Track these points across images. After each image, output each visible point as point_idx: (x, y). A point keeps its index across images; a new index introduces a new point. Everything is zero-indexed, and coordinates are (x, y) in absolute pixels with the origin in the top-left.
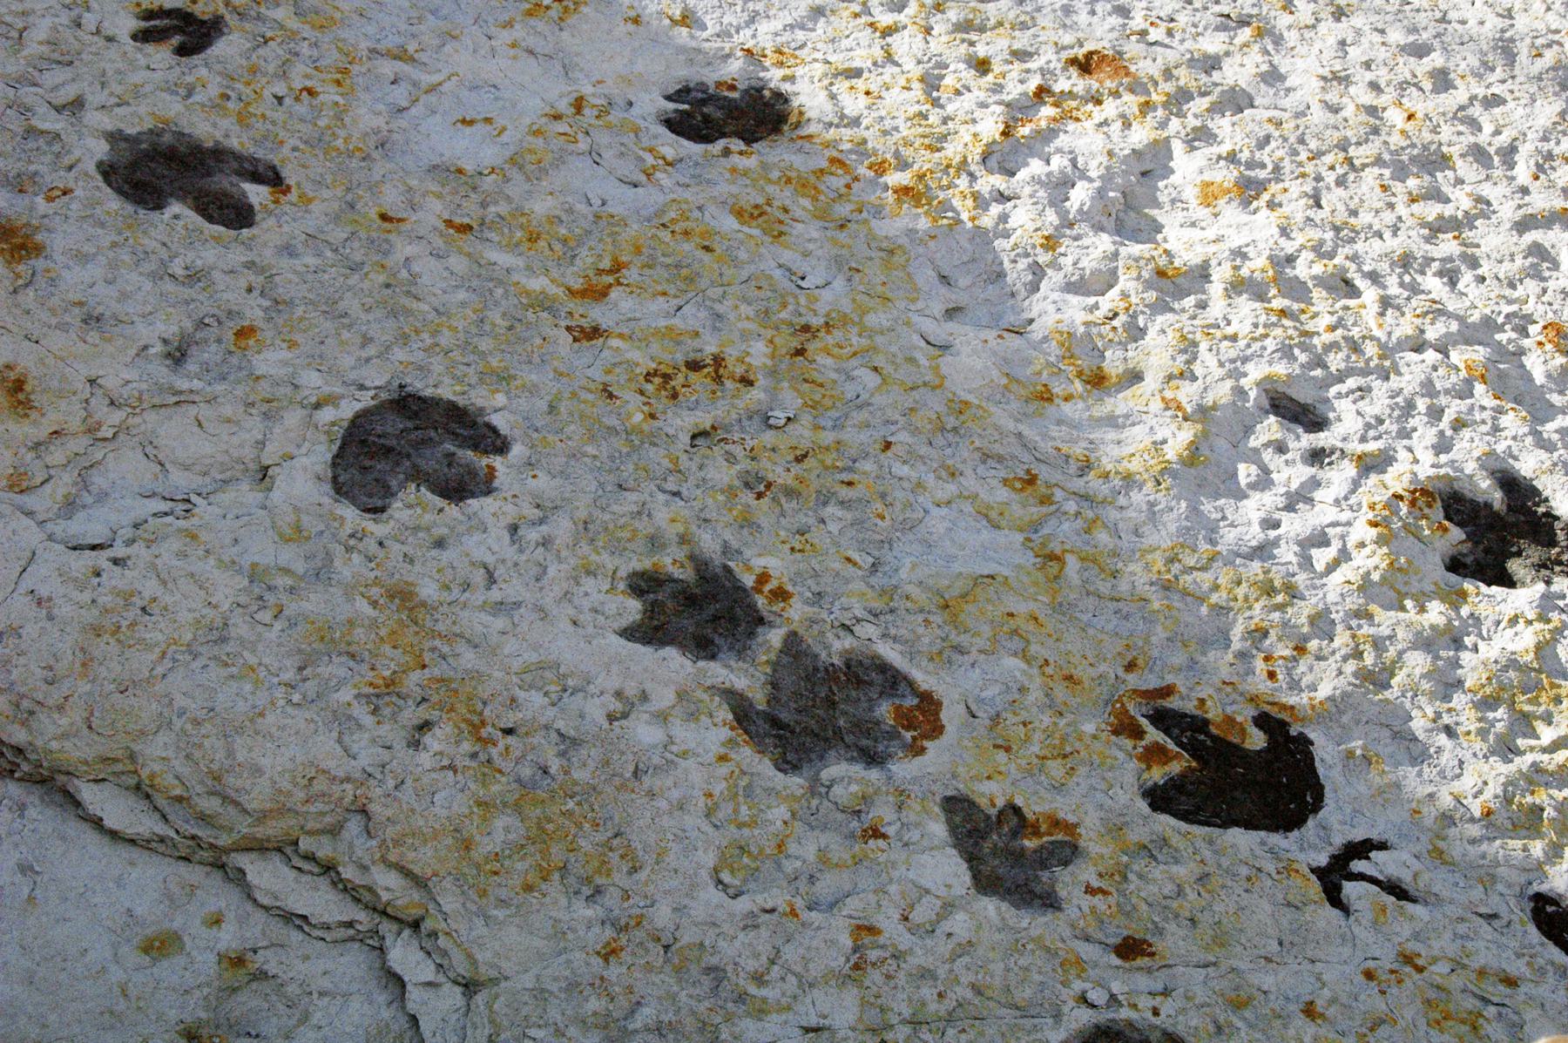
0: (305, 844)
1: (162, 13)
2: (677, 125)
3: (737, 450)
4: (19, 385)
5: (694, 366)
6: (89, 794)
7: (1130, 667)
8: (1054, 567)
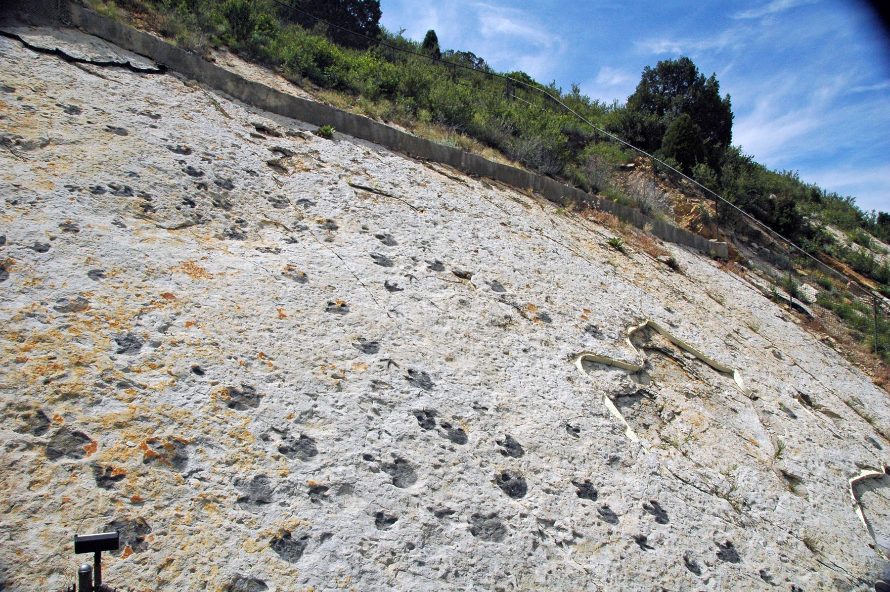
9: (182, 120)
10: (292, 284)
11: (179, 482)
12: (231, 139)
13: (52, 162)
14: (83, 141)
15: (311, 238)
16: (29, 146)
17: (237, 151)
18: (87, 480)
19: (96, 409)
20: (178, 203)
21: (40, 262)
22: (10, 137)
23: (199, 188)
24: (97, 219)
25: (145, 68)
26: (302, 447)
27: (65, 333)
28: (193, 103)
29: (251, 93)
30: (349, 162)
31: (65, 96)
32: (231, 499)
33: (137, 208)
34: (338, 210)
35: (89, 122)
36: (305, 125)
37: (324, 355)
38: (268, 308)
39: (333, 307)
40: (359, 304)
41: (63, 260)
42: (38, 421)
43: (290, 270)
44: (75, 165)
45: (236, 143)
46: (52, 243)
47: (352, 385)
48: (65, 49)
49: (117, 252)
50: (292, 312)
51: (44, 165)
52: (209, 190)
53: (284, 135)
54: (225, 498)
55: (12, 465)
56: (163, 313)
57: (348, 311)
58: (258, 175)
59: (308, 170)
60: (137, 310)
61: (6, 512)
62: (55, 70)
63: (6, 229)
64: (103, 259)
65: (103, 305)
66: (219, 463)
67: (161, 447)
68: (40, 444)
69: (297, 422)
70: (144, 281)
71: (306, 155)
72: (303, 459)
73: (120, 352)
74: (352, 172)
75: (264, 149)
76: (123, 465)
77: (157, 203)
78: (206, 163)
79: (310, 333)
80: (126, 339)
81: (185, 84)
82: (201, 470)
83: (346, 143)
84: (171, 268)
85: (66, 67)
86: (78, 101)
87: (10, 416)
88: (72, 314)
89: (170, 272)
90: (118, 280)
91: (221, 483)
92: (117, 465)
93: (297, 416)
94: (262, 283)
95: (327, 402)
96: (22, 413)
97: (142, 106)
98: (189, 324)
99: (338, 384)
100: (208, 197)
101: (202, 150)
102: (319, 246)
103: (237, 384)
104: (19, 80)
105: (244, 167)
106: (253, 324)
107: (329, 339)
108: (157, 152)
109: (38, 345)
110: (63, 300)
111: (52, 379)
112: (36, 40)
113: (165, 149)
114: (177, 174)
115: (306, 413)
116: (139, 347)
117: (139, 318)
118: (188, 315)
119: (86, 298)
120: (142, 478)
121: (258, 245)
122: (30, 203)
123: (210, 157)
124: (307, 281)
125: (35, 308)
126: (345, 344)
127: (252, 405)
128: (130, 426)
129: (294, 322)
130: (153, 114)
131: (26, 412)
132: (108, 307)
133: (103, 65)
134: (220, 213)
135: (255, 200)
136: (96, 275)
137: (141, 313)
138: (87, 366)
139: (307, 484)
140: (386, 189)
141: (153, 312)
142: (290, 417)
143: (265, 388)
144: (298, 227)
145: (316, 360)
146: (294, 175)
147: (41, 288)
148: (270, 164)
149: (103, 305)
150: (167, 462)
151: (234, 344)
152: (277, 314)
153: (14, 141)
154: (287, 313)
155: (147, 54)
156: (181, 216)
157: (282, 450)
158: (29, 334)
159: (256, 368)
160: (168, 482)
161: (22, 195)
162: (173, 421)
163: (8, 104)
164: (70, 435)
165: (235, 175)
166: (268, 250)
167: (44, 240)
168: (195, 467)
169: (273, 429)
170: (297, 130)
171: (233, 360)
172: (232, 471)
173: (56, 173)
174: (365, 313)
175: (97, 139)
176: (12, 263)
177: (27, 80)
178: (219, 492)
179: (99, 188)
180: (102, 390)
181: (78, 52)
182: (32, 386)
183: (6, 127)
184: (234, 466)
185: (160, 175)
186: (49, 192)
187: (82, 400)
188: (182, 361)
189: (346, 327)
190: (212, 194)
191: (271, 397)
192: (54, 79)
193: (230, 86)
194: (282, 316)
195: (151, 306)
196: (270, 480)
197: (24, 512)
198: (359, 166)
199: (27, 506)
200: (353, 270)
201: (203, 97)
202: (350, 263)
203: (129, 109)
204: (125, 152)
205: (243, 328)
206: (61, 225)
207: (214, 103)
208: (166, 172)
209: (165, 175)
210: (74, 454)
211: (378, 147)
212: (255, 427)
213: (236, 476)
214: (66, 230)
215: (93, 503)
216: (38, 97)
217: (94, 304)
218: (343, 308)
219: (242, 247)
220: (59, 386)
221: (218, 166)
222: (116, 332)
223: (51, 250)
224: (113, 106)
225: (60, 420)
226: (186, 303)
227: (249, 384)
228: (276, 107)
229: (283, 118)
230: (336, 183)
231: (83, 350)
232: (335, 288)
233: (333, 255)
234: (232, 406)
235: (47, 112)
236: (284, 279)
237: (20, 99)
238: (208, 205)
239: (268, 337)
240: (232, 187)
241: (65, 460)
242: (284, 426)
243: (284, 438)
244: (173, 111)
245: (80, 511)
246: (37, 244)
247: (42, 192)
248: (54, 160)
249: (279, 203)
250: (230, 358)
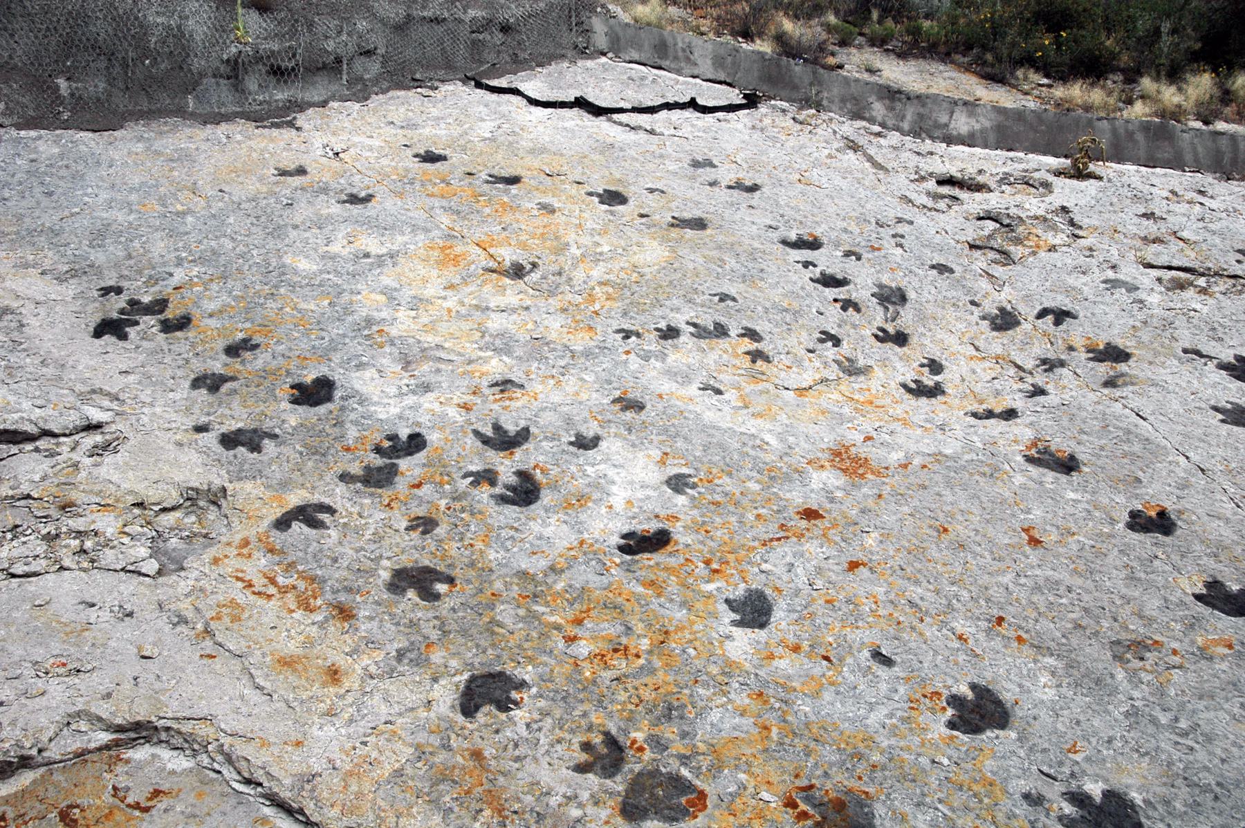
1: (418, 518)
2: (623, 549)
3: (629, 686)
4: (336, 672)
5: (616, 651)
7: (797, 776)
8: (765, 733)
29: (921, 116)
53: (993, 185)
59: (1052, 249)
112: (534, 85)
155: (722, 77)
156: (818, 364)
193: (878, 109)
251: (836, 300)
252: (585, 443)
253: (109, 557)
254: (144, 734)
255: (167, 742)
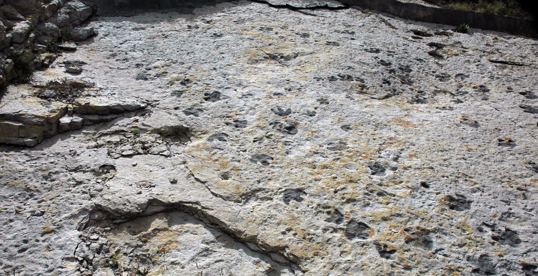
0: (279, 251)
6: (248, 244)
9: (368, 34)
10: (470, 130)
11: (431, 256)
12: (401, 41)
13: (302, 65)
14: (316, 52)
15: (472, 99)
16: (288, 58)
17: (407, 48)
18: (373, 252)
19: (368, 209)
20: (380, 83)
21: (313, 122)
22: (276, 55)
23: (390, 73)
24: (337, 95)
25: (336, 6)
26: (509, 237)
27: (338, 163)
28: (371, 23)
30: (485, 46)
31: (299, 28)
32: (468, 270)
33: (357, 88)
34: (486, 79)
35: (316, 41)
36: (446, 27)
37: (507, 174)
38: (459, 145)
39: (502, 142)
40: (522, 140)
41: (325, 121)
42: (336, 215)
43: (465, 120)
44: (316, 66)
45: (405, 43)
46: (316, 111)
47: (534, 195)
48: (290, 4)
49: (354, 114)
50: (475, 147)
51: (299, 68)
52: (397, 73)
54: (463, 268)
55: (328, 241)
56: (393, 150)
57: (515, 145)
58: (425, 62)
59: (457, 55)
60: (376, 148)
61: (332, 269)
62: (288, 16)
63: (289, 105)
64: (348, 119)
65: (356, 146)
66: (454, 245)
67: (414, 234)
68: (341, 229)
69: (500, 219)
70: (375, 130)
71: (452, 46)
72: (512, 245)
73: (373, 174)
74: (488, 52)
75: (424, 44)
76: (394, 244)
77: (369, 83)
78: (390, 58)
79: (492, 160)
80: (375, 166)
81: (362, 12)
82: (443, 249)
83: (478, 35)
84: (389, 122)
85: (293, 14)
86: (306, 30)
87: (320, 212)
88: (339, 151)
89: (388, 124)
90: (360, 130)
91: (458, 258)
92: (389, 243)
93: (499, 215)
94: (449, 129)
95: (519, 206)
96: (326, 210)
97: (342, 28)
98: (411, 156)
99: (524, 194)
100: (397, 78)
101: (386, 49)
102: (479, 103)
103: (452, 193)
104: (273, 24)
105: (415, 57)
106: (452, 155)
107: (508, 164)
108: (360, 53)
109: (324, 170)
110: (331, 143)
111: (338, 190)
113: (363, 51)
114: (375, 65)
115: (505, 214)
116: (383, 170)
117: (379, 153)
118: (409, 150)
119: (344, 142)
120: (406, 253)
121: (437, 106)
122: (298, 89)
123: (392, 53)
124: (479, 126)
125: (317, 148)
126: (520, 167)
127: (466, 208)
128: (391, 219)
129: (479, 153)
130: (350, 32)
131: (328, 210)
132: (359, 147)
133: (313, 9)
134: (407, 87)
135: (427, 77)
136: (346, 128)
137: (380, 150)
138: (356, 182)
139: (520, 263)
140: (518, 60)
141: (387, 149)
142: (495, 216)
143: (472, 196)
144: (460, 92)
145: (502, 178)
146: (450, 59)
147: (317, 137)
148: (431, 54)
149: (356, 146)
150: (419, 243)
151: (443, 168)
152: (465, 148)
153: (279, 56)
154: (473, 148)
156: (384, 91)
157: (494, 238)
158: (318, 164)
159: (462, 183)
160: (424, 256)
161: (292, 85)
162: (417, 217)
163: (271, 37)
164: (356, 224)
165: (410, 63)
166: (444, 108)
167: (312, 109)
168: (439, 247)
169: (484, 224)
170: (441, 31)
171: (445, 178)
172: (464, 251)
173: (307, 71)
174: (529, 145)
175: (323, 49)
176: (297, 124)
177: (277, 23)
178: (458, 265)
179: (333, 77)
180: (369, 197)
181: (298, 4)
182: (328, 194)
183: (273, 49)
184: (464, 248)
185: (365, 67)
186: (306, 82)
187: (358, 203)
188: (413, 179)
189: (517, 155)
190: (399, 76)
191: (478, 202)
192: (290, 20)
194: (469, 150)
195: (384, 145)
196: (492, 258)
197: (341, 270)
198: (492, 48)
199: (342, 266)
200: (510, 117)
201: (375, 18)
202: (506, 113)
203: (335, 31)
204: (341, 55)
205: (446, 157)
206: (318, 100)
207: (383, 21)
208: (368, 65)
209: (368, 66)
210: (362, 236)
211: (502, 33)
212: (471, 222)
213: (467, 255)
214: (321, 103)
215: (380, 267)
216: (285, 31)
217: (350, 145)
218: (511, 143)
219: (427, 108)
220: (343, 194)
221: (398, 58)
222: (368, 161)
223: (317, 115)
224: (326, 30)
225: (349, 215)
226: (405, 143)
227: (460, 194)
228: (424, 17)
229: (430, 24)
230: (479, 61)
231: (352, 173)
232: (500, 130)
233: (492, 108)
234: (452, 208)
235: (292, 38)
236: (463, 126)
237: (276, 33)
238: (398, 83)
239: (464, 163)
240: (411, 71)
241: (357, 240)
242: (492, 222)
243: (493, 231)
244: (361, 29)
245: (374, 271)
246: (308, 112)
247: (303, 83)
248: (303, 64)
249: (443, 78)
250: (443, 177)
251: (387, 70)
252: (312, 115)
253: (154, 149)
254: (175, 207)
255: (183, 210)
